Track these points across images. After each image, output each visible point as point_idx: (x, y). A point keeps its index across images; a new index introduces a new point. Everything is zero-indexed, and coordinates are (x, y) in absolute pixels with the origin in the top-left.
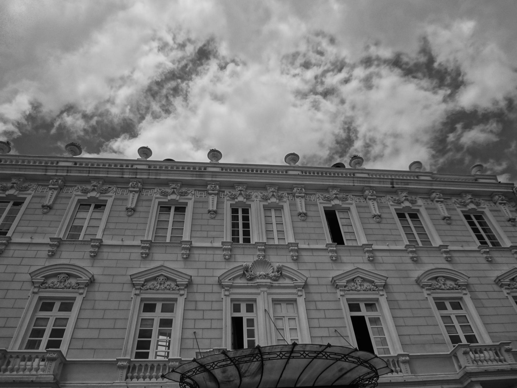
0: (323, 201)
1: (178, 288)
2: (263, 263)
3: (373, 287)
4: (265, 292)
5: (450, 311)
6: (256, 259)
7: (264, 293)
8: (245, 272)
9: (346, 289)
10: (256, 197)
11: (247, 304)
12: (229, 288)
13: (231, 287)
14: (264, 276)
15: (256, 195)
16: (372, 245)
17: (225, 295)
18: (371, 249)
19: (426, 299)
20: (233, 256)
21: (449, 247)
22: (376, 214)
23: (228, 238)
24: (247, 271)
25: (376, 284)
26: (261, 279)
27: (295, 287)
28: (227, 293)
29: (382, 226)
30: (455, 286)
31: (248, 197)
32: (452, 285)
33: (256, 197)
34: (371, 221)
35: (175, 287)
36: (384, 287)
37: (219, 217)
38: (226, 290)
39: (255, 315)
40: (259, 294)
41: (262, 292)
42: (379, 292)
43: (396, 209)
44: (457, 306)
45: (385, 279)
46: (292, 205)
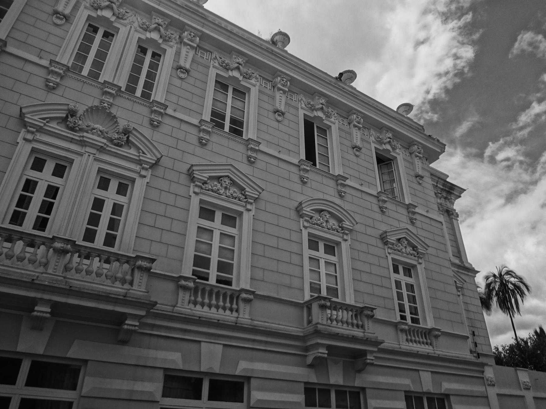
0: (219, 67)
3: (240, 195)
4: (92, 156)
5: (321, 253)
6: (96, 103)
7: (89, 155)
8: (69, 116)
11: (56, 164)
12: (34, 130)
13: (40, 130)
16: (261, 143)
17: (25, 139)
18: (257, 148)
19: (300, 231)
21: (347, 181)
22: (279, 109)
25: (247, 193)
26: (93, 134)
28: (29, 137)
29: (281, 127)
30: (338, 227)
32: (334, 225)
34: (271, 115)
36: (254, 200)
38: (29, 131)
39: (63, 183)
40: (81, 155)
41: (87, 154)
42: (246, 205)
43: (305, 115)
44: (330, 249)
45: (261, 191)
46: (178, 54)
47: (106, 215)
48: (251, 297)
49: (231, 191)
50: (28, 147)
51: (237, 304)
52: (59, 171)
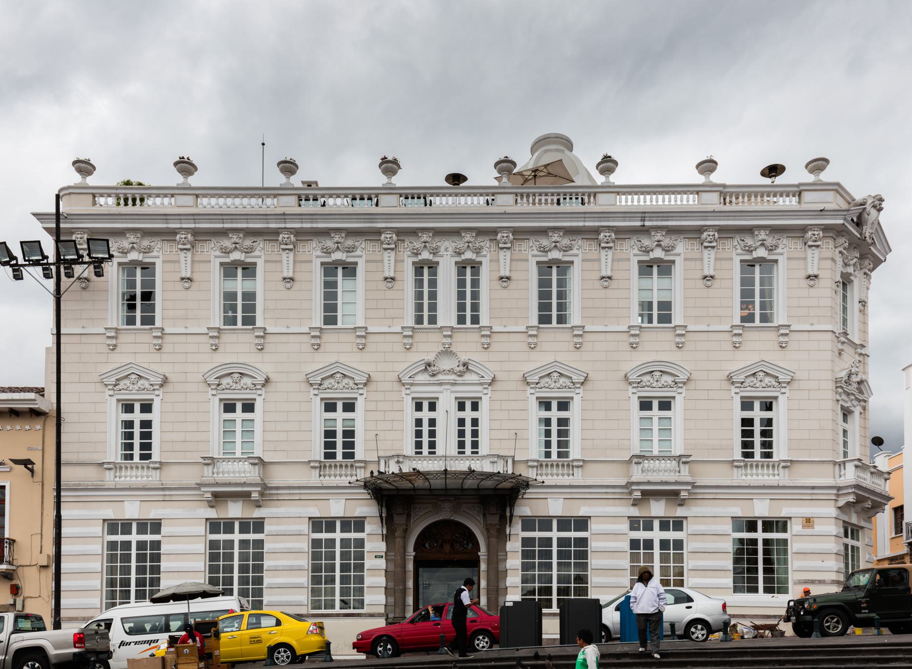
1: (356, 387)
2: (447, 352)
6: (441, 348)
8: (428, 367)
9: (537, 386)
10: (446, 250)
14: (448, 372)
15: (447, 246)
20: (415, 344)
23: (410, 321)
24: (429, 366)
27: (481, 384)
28: (408, 392)
31: (435, 252)
33: (446, 250)
35: (354, 385)
37: (397, 285)
47: (468, 428)
48: (581, 463)
49: (561, 382)
50: (410, 398)
51: (573, 470)
52: (432, 407)
